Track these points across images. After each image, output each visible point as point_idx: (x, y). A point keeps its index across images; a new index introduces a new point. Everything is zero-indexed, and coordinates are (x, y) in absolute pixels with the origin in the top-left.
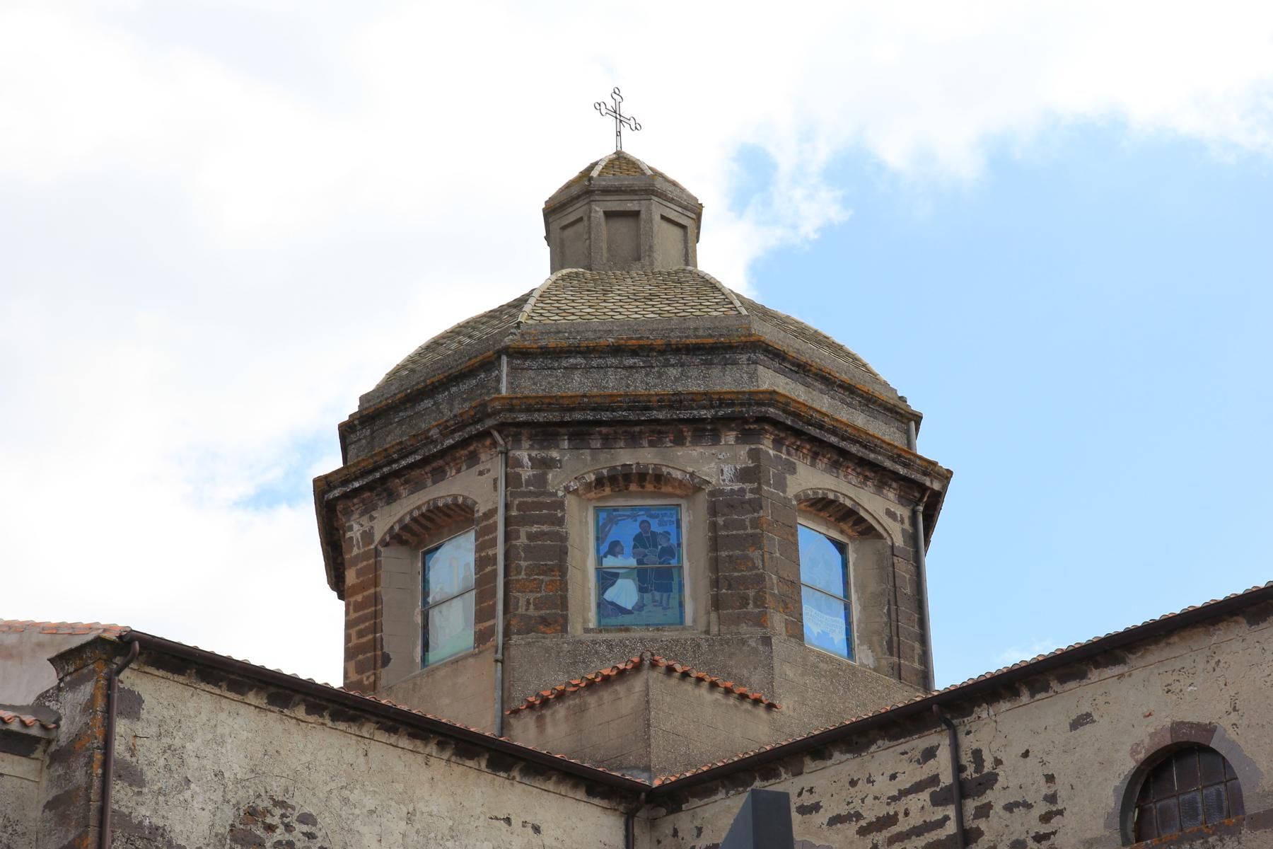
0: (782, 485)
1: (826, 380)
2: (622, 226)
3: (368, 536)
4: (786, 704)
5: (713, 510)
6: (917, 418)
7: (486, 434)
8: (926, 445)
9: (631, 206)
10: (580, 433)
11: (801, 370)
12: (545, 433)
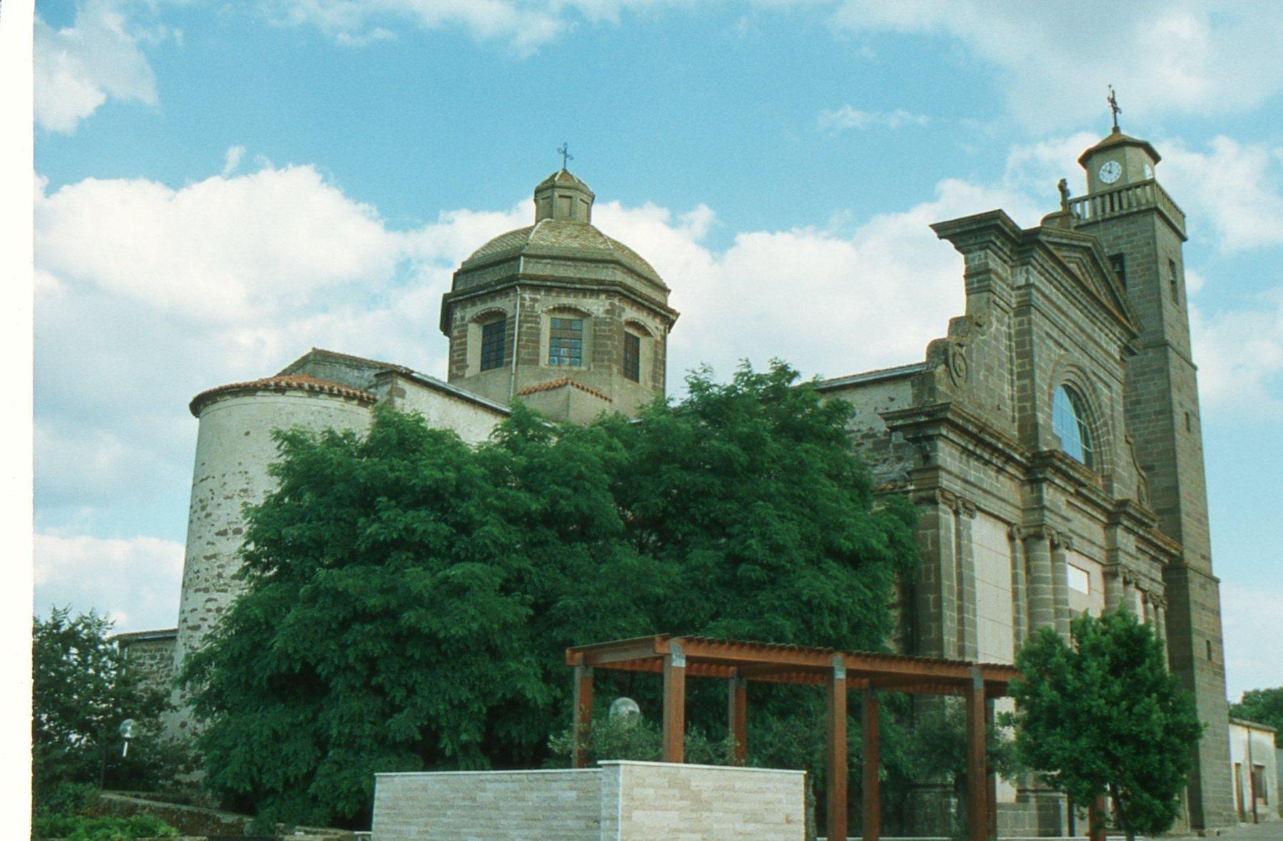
0: (620, 316)
1: (640, 276)
2: (566, 202)
3: (463, 318)
4: (615, 400)
5: (595, 325)
6: (669, 291)
7: (513, 287)
8: (672, 302)
9: (568, 193)
10: (549, 289)
11: (630, 271)
12: (535, 288)
